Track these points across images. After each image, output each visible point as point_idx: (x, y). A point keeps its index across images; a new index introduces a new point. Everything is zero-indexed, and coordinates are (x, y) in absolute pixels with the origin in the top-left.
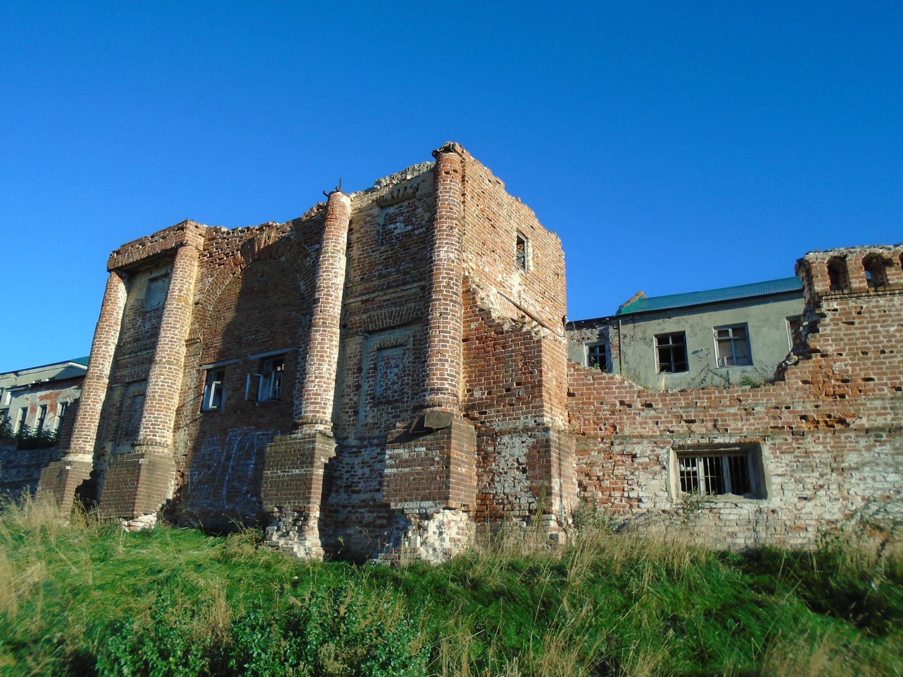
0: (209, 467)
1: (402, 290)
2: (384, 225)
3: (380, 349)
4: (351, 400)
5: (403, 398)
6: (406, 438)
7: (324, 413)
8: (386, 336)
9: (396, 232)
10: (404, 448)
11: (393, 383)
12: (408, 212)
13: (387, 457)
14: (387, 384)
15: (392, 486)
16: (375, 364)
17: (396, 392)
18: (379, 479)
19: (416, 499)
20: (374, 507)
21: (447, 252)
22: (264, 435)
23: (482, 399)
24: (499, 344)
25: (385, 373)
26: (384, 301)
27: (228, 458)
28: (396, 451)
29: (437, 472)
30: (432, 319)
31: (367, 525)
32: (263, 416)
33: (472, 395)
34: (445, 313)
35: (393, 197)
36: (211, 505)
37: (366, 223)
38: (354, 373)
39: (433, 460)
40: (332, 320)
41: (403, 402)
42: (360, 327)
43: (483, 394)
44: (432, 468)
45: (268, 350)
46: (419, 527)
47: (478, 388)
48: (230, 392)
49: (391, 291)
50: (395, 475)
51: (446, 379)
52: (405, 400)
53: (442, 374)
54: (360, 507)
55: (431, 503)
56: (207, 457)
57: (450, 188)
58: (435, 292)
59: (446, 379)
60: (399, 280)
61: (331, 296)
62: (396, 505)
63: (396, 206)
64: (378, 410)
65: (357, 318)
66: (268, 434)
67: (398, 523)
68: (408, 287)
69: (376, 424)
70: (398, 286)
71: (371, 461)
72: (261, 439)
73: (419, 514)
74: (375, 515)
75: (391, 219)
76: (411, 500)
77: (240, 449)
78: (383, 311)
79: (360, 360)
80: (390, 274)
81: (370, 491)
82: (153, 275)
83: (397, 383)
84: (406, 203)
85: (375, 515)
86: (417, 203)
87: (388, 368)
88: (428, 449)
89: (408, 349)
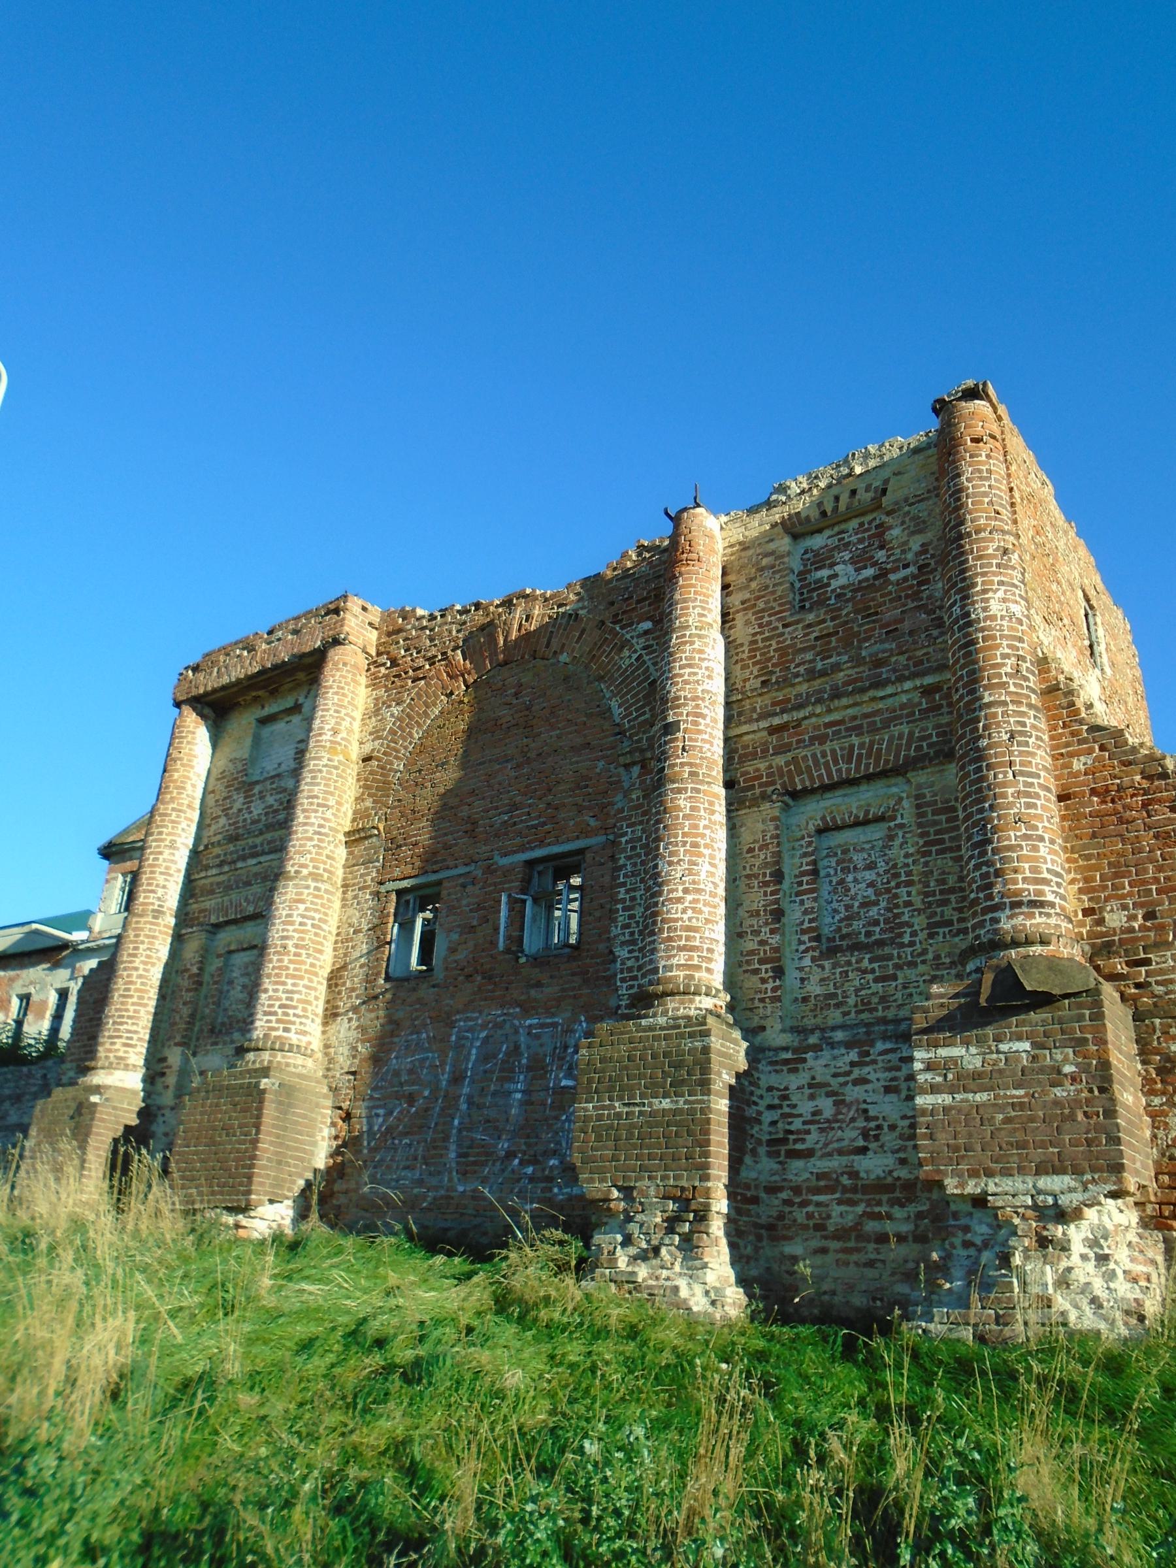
0: (411, 1099)
1: (873, 699)
2: (800, 573)
3: (820, 831)
4: (762, 943)
5: (901, 935)
6: (968, 1018)
7: (708, 970)
8: (839, 800)
9: (835, 584)
10: (966, 1043)
11: (866, 904)
12: (861, 541)
13: (918, 1066)
14: (848, 907)
15: (943, 1138)
16: (814, 862)
17: (876, 923)
18: (861, 1123)
19: (1021, 1170)
20: (854, 1190)
21: (1004, 600)
22: (542, 1026)
23: (1131, 930)
24: (1160, 801)
25: (842, 882)
26: (828, 725)
27: (457, 1079)
28: (943, 1052)
29: (1075, 1103)
30: (989, 747)
31: (841, 1234)
32: (539, 985)
33: (1101, 922)
34: (1022, 733)
35: (824, 514)
36: (420, 1182)
37: (762, 569)
38: (766, 884)
39: (1059, 1072)
40: (710, 768)
41: (902, 945)
42: (773, 783)
43: (1132, 918)
44: (1059, 1092)
45: (542, 843)
46: (1043, 1242)
47: (1115, 904)
48: (455, 936)
49: (845, 701)
50: (946, 1110)
51: (1046, 882)
52: (907, 939)
53: (1034, 870)
54: (818, 1191)
55: (1067, 1180)
56: (404, 1078)
57: (990, 471)
58: (986, 688)
59: (1046, 882)
60: (860, 679)
61: (704, 716)
62: (962, 1185)
63: (827, 533)
65: (762, 766)
66: (554, 1025)
67: (966, 1229)
68: (889, 690)
69: (834, 995)
70: (863, 690)
71: (835, 1083)
72: (538, 1037)
73: (1035, 1207)
74: (860, 1209)
75: (820, 559)
76: (1006, 1173)
77: (485, 1058)
78: (827, 747)
79: (778, 855)
80: (836, 668)
81: (841, 1152)
82: (269, 710)
83: (876, 903)
84: (854, 524)
85: (860, 1209)
86: (889, 520)
87: (846, 870)
88: (1034, 1045)
89: (901, 826)
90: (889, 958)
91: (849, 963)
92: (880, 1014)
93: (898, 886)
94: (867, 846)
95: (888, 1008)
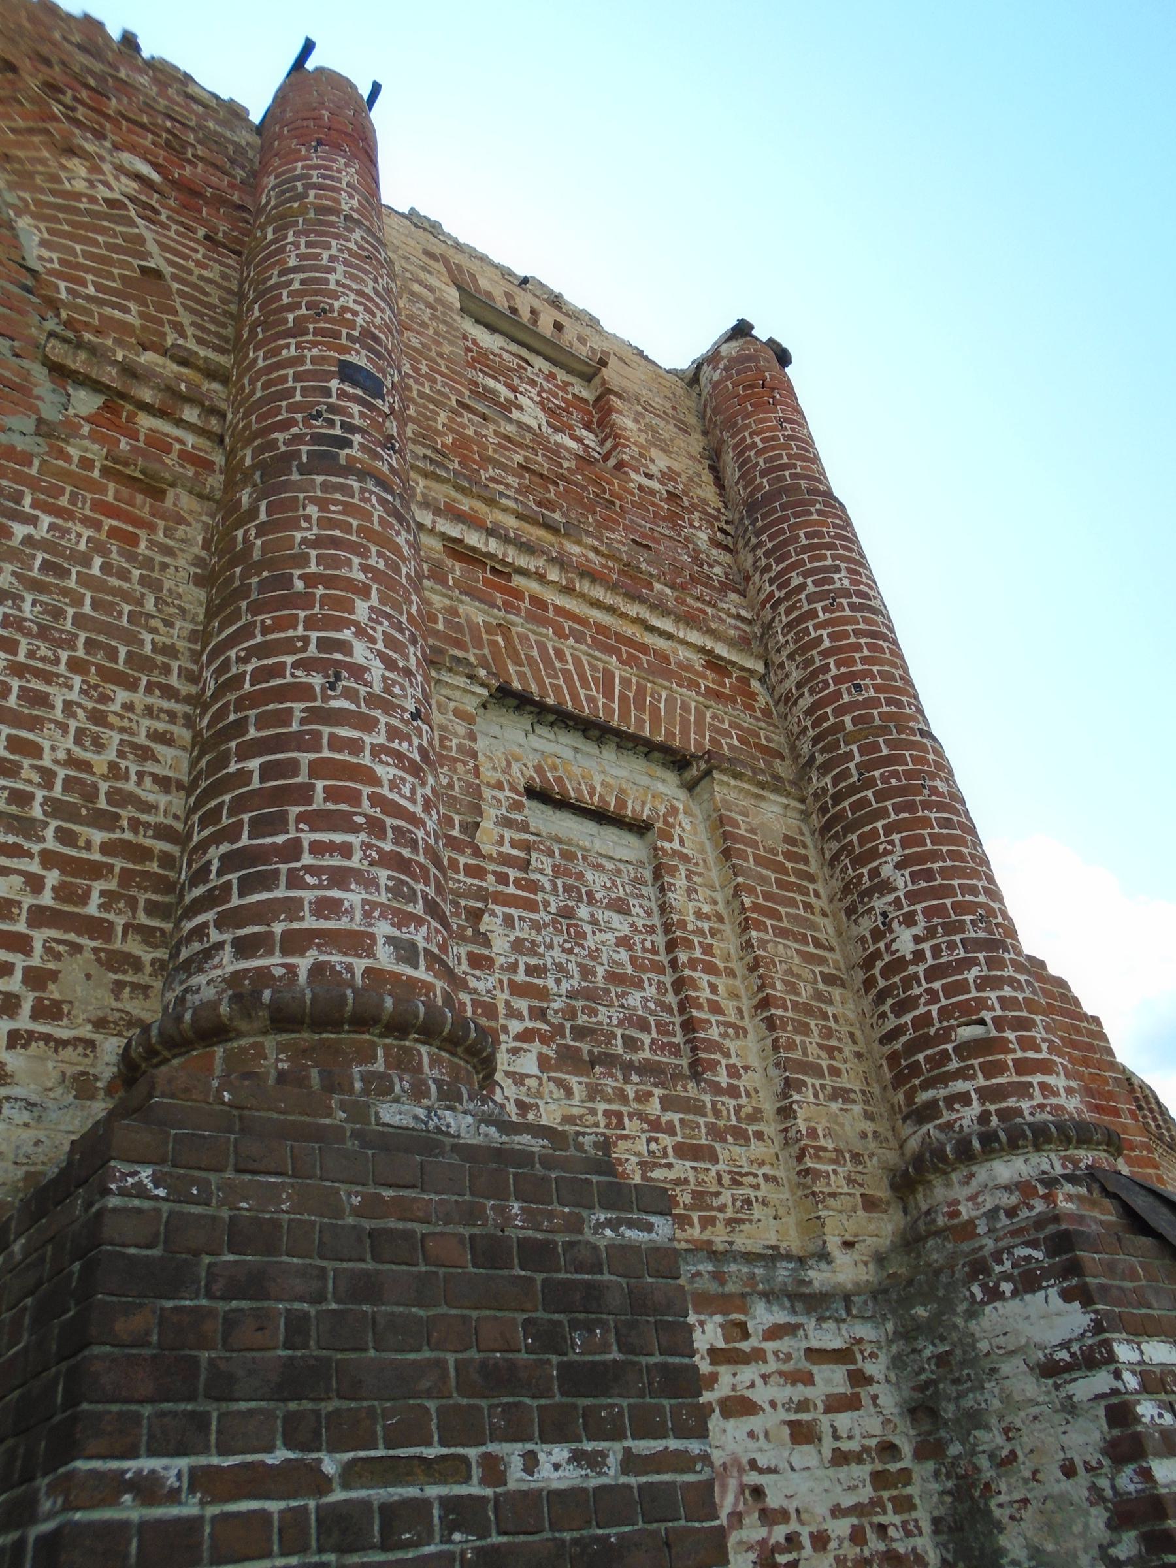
3: (532, 792)
14: (586, 972)
25: (567, 913)
49: (598, 593)
64: (594, 1092)
90: (700, 1110)
91: (622, 1097)
92: (695, 1232)
93: (693, 964)
94: (609, 866)
95: (712, 1221)
